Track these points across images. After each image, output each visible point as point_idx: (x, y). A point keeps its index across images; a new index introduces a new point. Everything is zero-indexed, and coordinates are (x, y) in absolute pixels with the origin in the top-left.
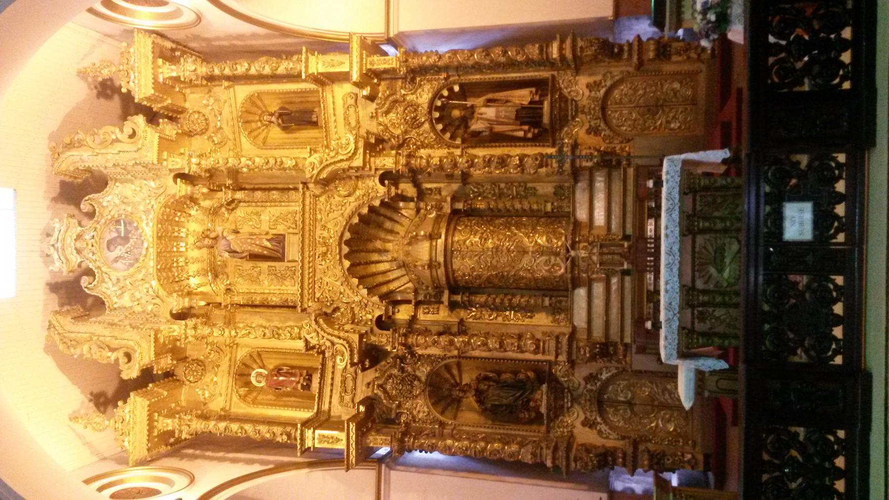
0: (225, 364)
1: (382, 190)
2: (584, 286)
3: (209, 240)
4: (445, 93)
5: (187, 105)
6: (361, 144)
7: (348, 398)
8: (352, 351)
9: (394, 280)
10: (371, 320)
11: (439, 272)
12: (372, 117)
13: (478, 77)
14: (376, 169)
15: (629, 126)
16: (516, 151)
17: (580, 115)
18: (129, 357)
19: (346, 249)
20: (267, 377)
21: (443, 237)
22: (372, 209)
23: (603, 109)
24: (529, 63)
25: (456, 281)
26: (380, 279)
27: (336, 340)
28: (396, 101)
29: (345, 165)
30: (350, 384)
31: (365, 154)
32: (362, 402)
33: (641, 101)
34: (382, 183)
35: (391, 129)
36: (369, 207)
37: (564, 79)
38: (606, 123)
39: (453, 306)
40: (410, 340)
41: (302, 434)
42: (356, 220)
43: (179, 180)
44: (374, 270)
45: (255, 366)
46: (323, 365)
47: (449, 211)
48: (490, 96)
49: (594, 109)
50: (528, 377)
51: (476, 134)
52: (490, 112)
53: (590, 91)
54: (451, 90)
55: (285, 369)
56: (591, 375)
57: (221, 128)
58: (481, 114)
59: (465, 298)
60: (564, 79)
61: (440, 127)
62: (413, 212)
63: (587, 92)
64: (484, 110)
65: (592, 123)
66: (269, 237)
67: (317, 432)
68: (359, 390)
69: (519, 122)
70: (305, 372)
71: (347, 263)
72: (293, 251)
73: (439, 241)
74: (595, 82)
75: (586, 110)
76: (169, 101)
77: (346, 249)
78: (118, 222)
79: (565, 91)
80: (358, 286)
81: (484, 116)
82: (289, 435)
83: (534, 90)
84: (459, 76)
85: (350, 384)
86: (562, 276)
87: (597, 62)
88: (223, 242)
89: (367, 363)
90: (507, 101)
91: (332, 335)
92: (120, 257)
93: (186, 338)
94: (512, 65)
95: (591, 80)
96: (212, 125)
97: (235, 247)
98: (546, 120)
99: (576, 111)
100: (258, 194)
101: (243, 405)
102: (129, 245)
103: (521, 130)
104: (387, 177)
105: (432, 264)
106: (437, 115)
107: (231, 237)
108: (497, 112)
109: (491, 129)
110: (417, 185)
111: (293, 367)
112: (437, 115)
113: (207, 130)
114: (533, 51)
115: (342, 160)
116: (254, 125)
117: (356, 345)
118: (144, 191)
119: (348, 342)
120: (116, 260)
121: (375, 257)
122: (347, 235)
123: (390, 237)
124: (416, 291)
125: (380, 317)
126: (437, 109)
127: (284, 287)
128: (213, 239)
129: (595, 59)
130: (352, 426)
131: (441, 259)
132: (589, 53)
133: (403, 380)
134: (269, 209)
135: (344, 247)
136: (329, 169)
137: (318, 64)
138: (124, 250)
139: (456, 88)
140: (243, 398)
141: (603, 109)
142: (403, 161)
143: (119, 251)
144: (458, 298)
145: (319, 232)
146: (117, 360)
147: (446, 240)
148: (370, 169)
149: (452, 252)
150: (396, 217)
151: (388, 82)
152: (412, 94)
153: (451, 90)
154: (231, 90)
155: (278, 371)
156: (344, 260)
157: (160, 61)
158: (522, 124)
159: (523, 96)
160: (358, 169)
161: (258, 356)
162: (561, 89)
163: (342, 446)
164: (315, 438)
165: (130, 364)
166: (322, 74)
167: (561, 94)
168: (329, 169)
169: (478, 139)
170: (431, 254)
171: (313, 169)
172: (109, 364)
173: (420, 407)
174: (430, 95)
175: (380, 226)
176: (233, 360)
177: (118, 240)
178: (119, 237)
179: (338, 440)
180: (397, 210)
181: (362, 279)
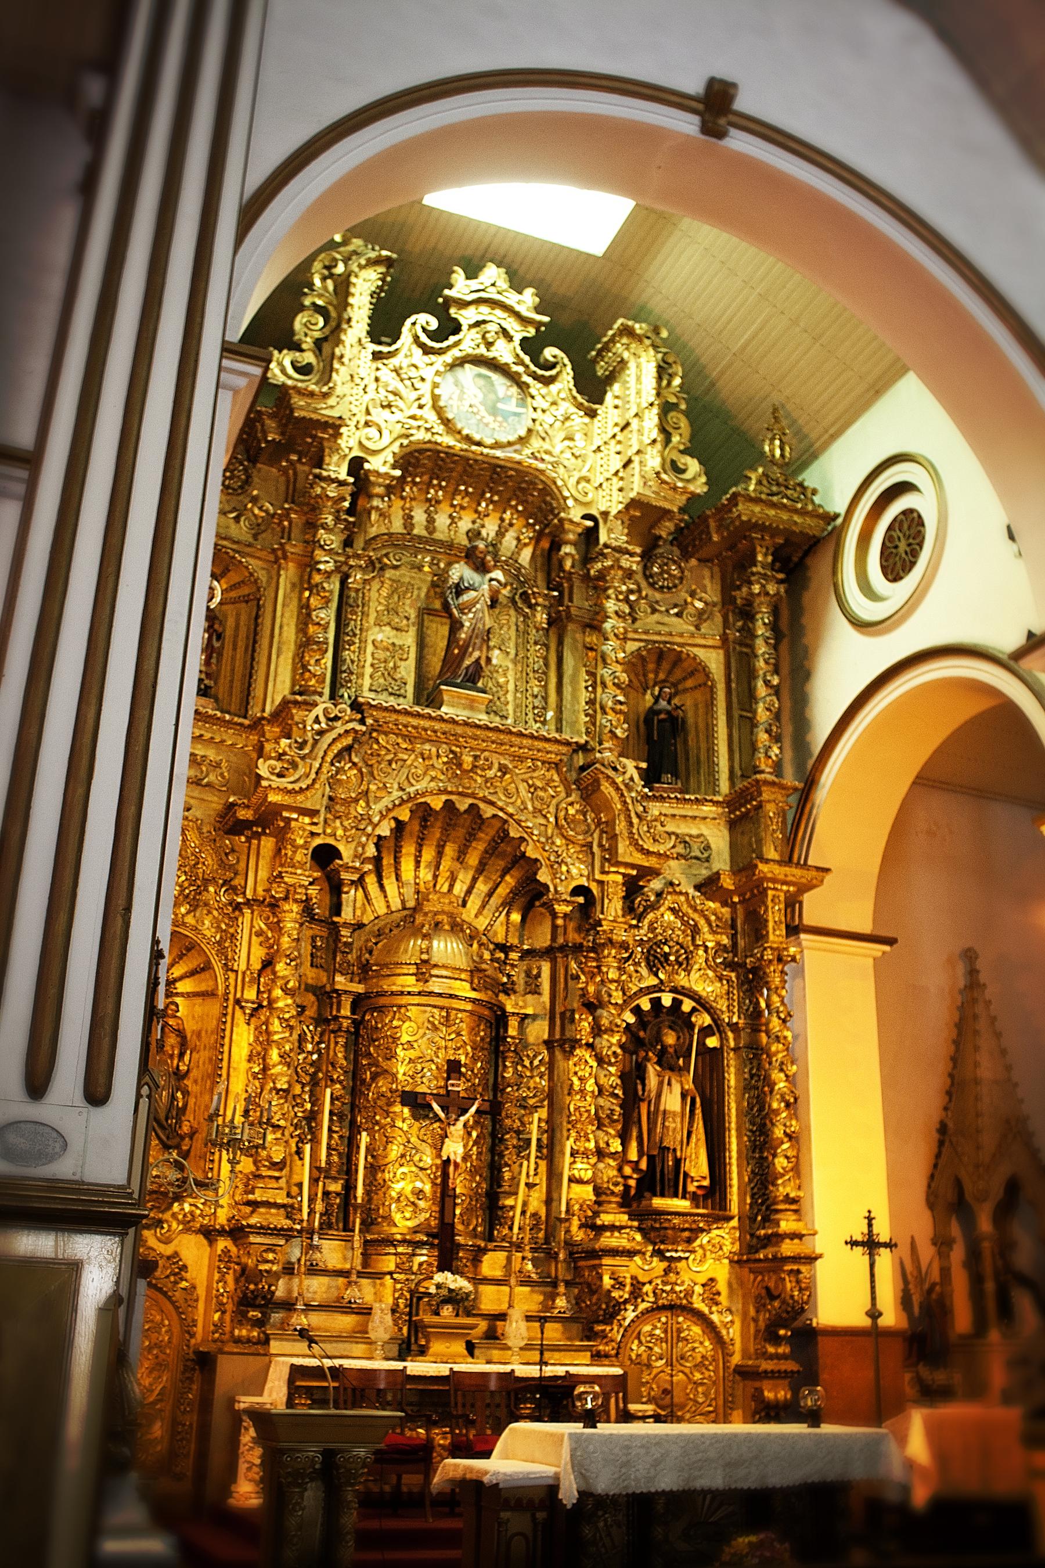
1: (565, 889)
2: (365, 1264)
4: (707, 1020)
5: (693, 562)
6: (651, 862)
8: (289, 792)
9: (382, 887)
10: (334, 835)
11: (412, 980)
12: (671, 884)
13: (732, 1083)
14: (601, 883)
15: (638, 1356)
17: (664, 1265)
18: (304, 370)
19: (463, 805)
21: (473, 995)
23: (671, 1308)
25: (381, 1009)
26: (387, 861)
28: (695, 930)
29: (621, 826)
31: (633, 866)
33: (681, 1376)
35: (651, 916)
36: (537, 860)
37: (724, 1237)
38: (648, 1310)
40: (295, 908)
43: (589, 523)
44: (404, 851)
47: (509, 1009)
48: (698, 1100)
49: (672, 1290)
50: (182, 1138)
52: (672, 1101)
53: (703, 1285)
54: (706, 1031)
55: (216, 644)
56: (184, 1268)
57: (654, 611)
58: (669, 1084)
59: (345, 1023)
61: (645, 1005)
62: (500, 939)
63: (702, 1279)
64: (677, 1089)
65: (647, 1288)
66: (483, 662)
69: (655, 1153)
70: (212, 683)
72: (455, 706)
73: (467, 985)
74: (719, 1293)
75: (672, 1277)
76: (715, 538)
77: (463, 805)
78: (522, 402)
79: (704, 1239)
80: (395, 819)
81: (665, 1086)
83: (706, 1183)
84: (735, 1050)
86: (388, 1219)
87: (758, 1298)
90: (689, 1134)
92: (462, 392)
95: (722, 1286)
96: (658, 596)
97: (466, 597)
98: (658, 1202)
99: (671, 1259)
102: (483, 412)
103: (640, 1156)
104: (587, 901)
105: (424, 969)
106: (667, 1000)
108: (674, 1113)
109: (643, 1100)
110: (549, 953)
112: (667, 1000)
113: (652, 585)
115: (631, 824)
116: (651, 666)
118: (573, 459)
119: (308, 788)
121: (428, 854)
123: (459, 889)
126: (677, 1004)
127: (368, 670)
131: (435, 986)
132: (788, 1285)
134: (511, 666)
135: (470, 801)
136: (616, 797)
138: (476, 402)
139: (712, 1042)
141: (671, 1308)
144: (346, 1011)
145: (496, 760)
146: (297, 347)
147: (465, 999)
148: (603, 872)
149: (442, 1008)
150: (495, 901)
151: (728, 916)
152: (707, 960)
153: (706, 1031)
154: (718, 643)
156: (444, 798)
157: (780, 541)
158: (651, 1159)
159: (697, 1166)
160: (613, 850)
162: (709, 1231)
165: (290, 371)
166: (760, 806)
167: (702, 1230)
170: (444, 967)
171: (615, 769)
172: (292, 332)
174: (704, 994)
175: (481, 869)
176: (248, 550)
177: (492, 396)
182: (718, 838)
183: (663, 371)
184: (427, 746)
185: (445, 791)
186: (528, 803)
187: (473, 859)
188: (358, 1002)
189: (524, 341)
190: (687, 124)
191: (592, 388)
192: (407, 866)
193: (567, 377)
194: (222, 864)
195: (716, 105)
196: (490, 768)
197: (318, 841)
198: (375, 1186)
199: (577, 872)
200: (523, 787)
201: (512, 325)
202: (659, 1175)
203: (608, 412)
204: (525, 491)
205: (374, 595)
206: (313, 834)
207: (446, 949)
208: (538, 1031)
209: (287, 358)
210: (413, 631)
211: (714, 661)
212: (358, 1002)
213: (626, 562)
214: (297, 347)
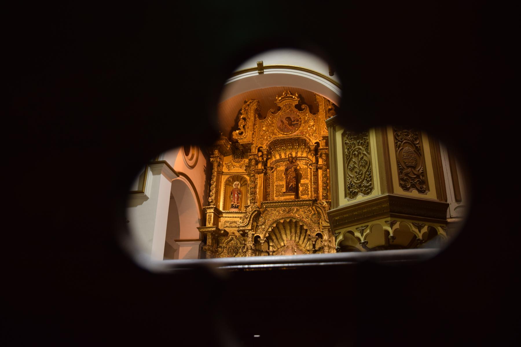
0: (242, 170)
7: (228, 224)
19: (288, 220)
20: (238, 188)
22: (306, 230)
27: (248, 219)
30: (233, 225)
32: (225, 231)
34: (316, 235)
40: (250, 251)
41: (212, 208)
42: (301, 224)
45: (242, 182)
46: (242, 213)
62: (308, 248)
67: (213, 214)
68: (231, 229)
71: (282, 221)
78: (298, 121)
82: (212, 202)
85: (233, 225)
88: (291, 165)
89: (241, 232)
91: (250, 218)
92: (283, 123)
93: (250, 155)
101: (225, 180)
104: (320, 236)
107: (293, 169)
111: (241, 199)
117: (246, 228)
119: (247, 225)
120: (282, 121)
121: (288, 232)
122: (294, 221)
125: (259, 237)
127: (275, 192)
128: (292, 161)
130: (214, 229)
133: (236, 248)
136: (321, 211)
142: (326, 244)
146: (240, 129)
150: (306, 240)
155: (240, 193)
163: (208, 225)
164: (210, 212)
168: (321, 211)
175: (301, 233)
178: (292, 122)
179: (209, 223)
180: (309, 240)
181: (277, 227)
184: (278, 209)
185: (282, 218)
187: (298, 231)
189: (297, 107)
190: (255, 73)
192: (284, 237)
194: (241, 243)
196: (293, 210)
197: (255, 235)
199: (317, 231)
200: (302, 213)
205: (275, 175)
206: (253, 234)
209: (238, 131)
210: (285, 180)
213: (324, 151)
214: (240, 129)
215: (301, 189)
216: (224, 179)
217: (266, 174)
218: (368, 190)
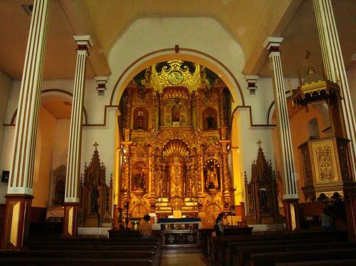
3: (177, 100)
16: (202, 182)
24: (224, 186)
37: (220, 194)
39: (162, 167)
51: (207, 172)
52: (212, 175)
60: (220, 194)
94: (224, 181)
100: (189, 112)
114: (227, 187)
124: (165, 157)
129: (224, 202)
137: (223, 130)
140: (135, 110)
143: (174, 76)
159: (216, 184)
161: (147, 113)
169: (205, 172)
173: (135, 159)
182: (218, 136)
183: (201, 66)
186: (185, 136)
188: (166, 167)
190: (174, 52)
191: (192, 70)
193: (188, 71)
195: (177, 49)
198: (170, 191)
199: (194, 146)
201: (178, 64)
202: (211, 185)
203: (195, 74)
204: (183, 89)
207: (176, 158)
208: (192, 167)
211: (217, 108)
212: (166, 167)
215: (181, 118)
216: (133, 109)
217: (160, 108)
218: (331, 176)
